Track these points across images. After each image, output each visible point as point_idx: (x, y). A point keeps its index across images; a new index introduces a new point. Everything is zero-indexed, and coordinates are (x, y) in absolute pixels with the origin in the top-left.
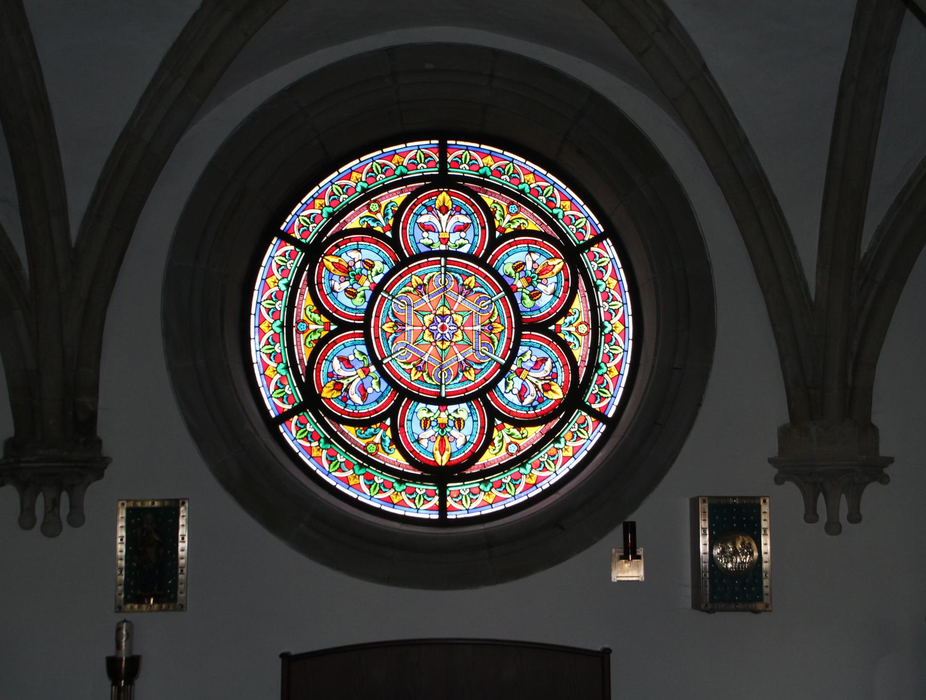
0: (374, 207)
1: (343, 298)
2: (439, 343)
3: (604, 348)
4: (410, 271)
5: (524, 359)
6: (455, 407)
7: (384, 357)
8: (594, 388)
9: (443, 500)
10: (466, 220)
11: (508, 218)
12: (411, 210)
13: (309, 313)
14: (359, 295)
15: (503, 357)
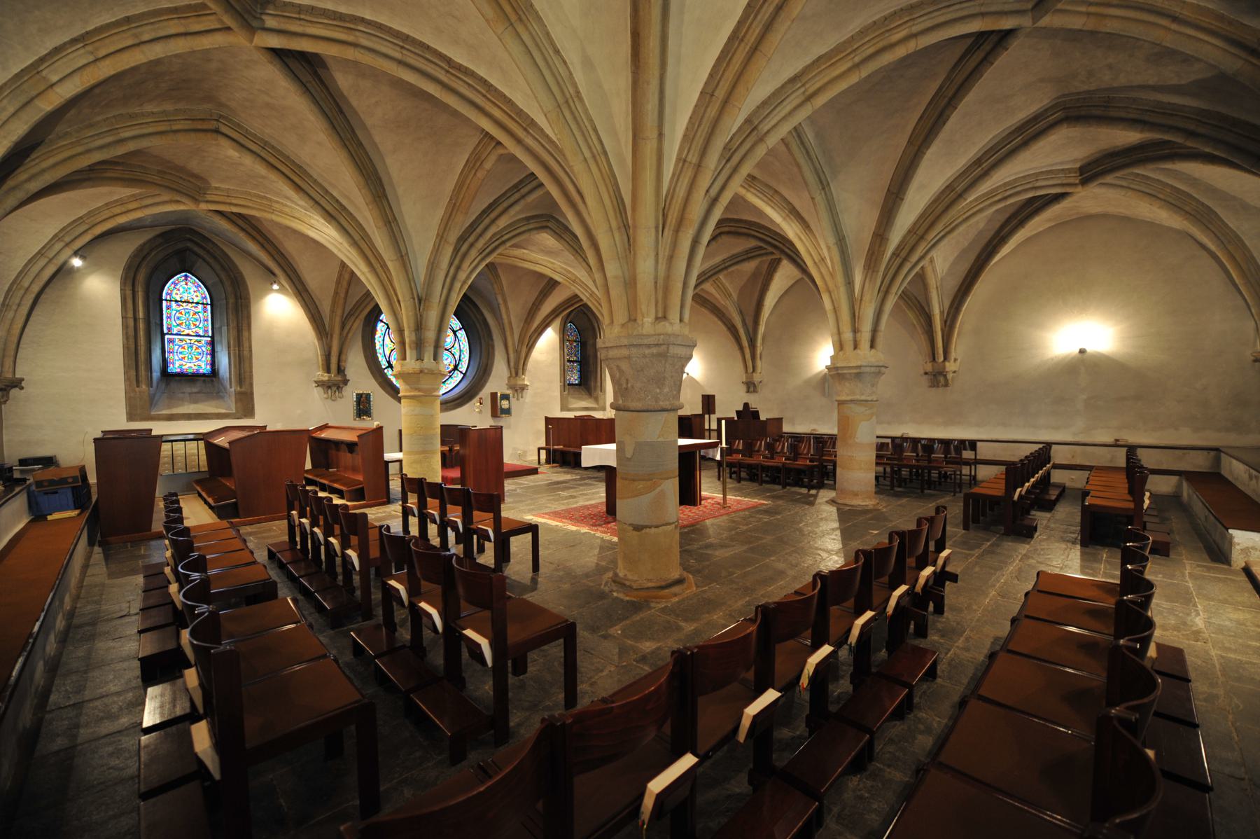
3: (462, 356)
8: (460, 366)
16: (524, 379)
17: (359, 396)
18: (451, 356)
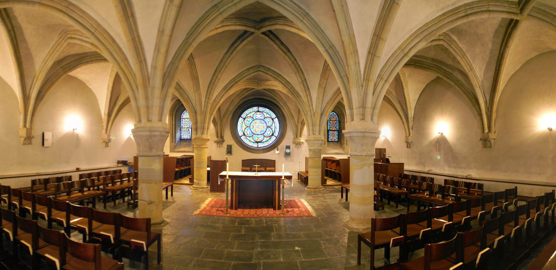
3: (276, 129)
8: (275, 134)
16: (300, 139)
17: (228, 146)
18: (270, 130)
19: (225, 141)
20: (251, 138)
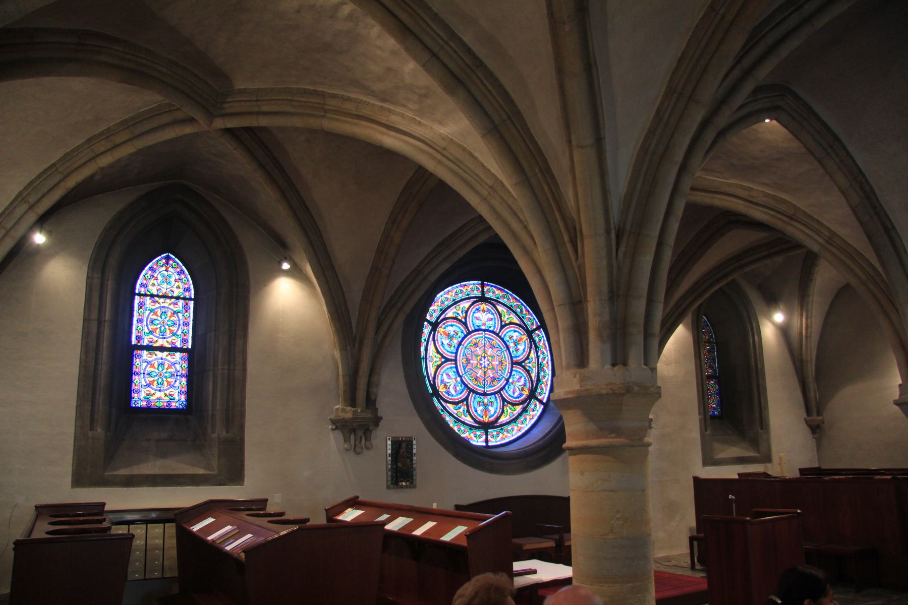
0: (458, 308)
1: (447, 347)
2: (483, 369)
4: (471, 337)
5: (514, 377)
6: (490, 397)
7: (463, 374)
8: (539, 390)
9: (487, 438)
10: (492, 316)
11: (507, 316)
12: (472, 310)
13: (434, 353)
14: (453, 346)
15: (507, 376)
19: (381, 418)
20: (463, 408)
